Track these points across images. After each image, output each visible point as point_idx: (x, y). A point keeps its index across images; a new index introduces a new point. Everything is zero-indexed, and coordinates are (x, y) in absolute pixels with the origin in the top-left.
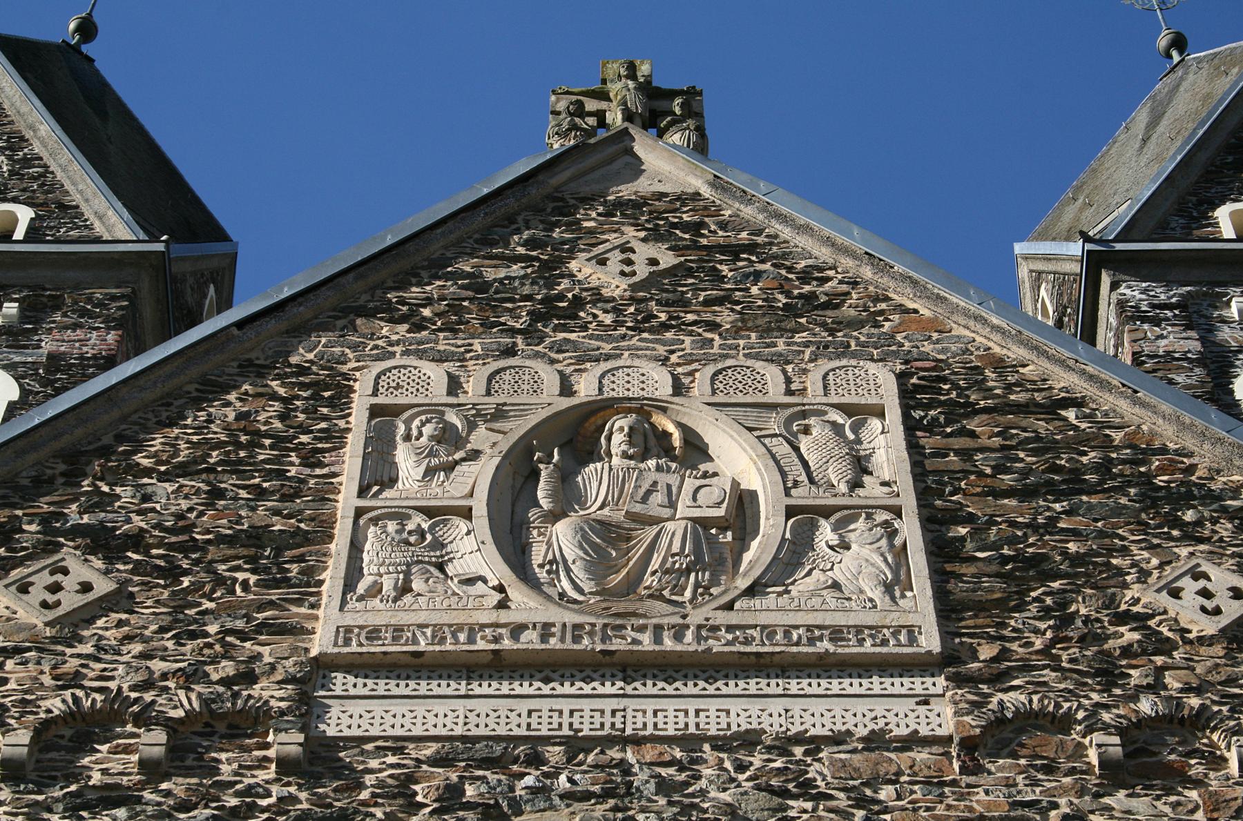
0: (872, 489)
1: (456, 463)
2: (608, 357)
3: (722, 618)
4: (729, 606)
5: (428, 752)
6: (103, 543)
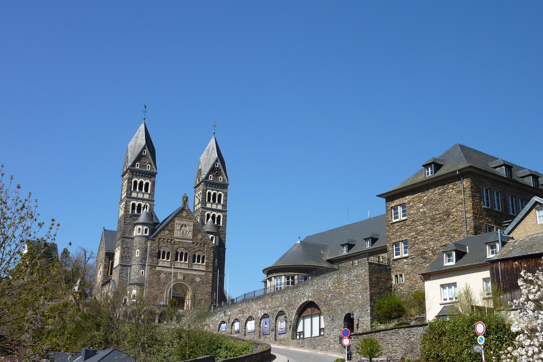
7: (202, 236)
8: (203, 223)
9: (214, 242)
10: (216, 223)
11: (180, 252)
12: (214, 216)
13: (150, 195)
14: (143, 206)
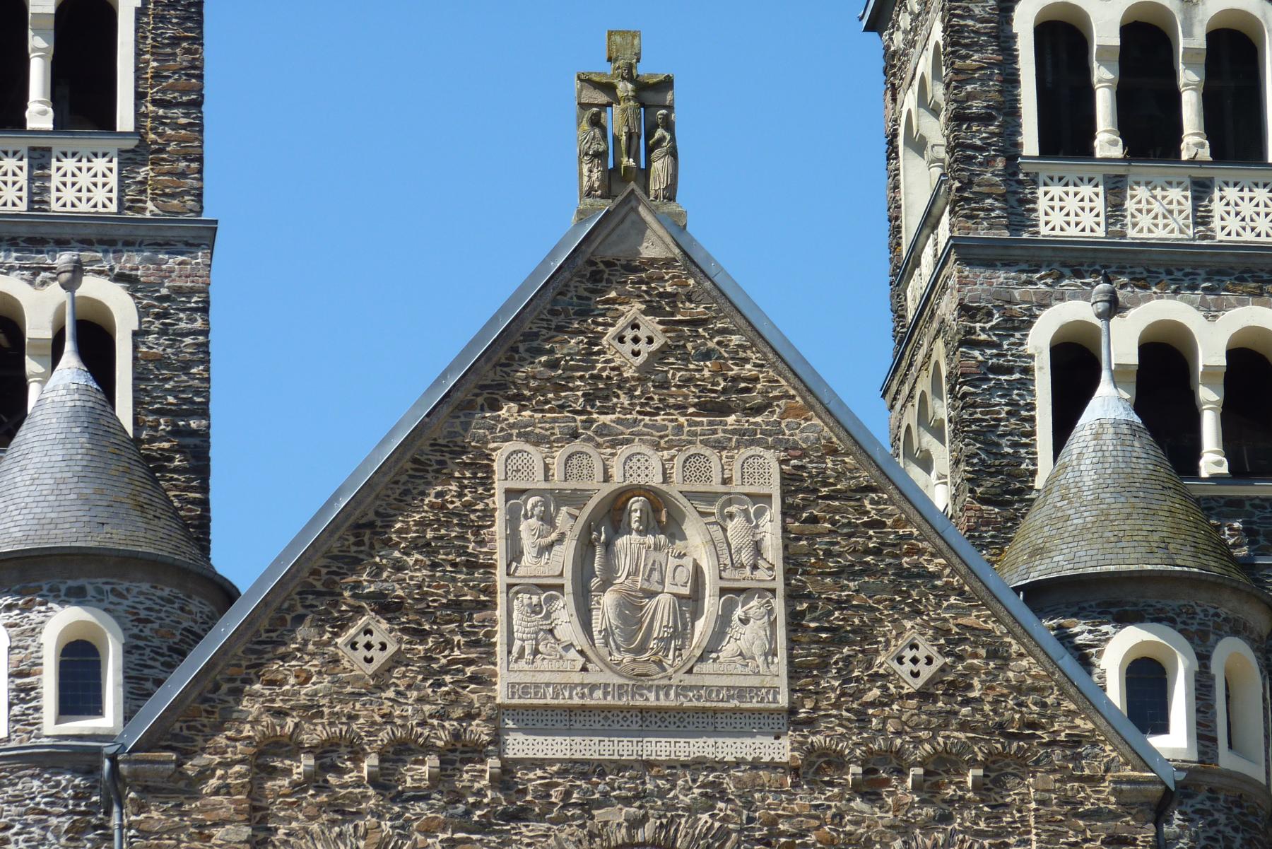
0: (761, 574)
1: (552, 545)
2: (628, 442)
3: (689, 680)
4: (690, 671)
5: (555, 768)
6: (387, 607)
7: (950, 642)
8: (1000, 486)
9: (1175, 741)
12: (1164, 362)
13: (129, 160)
14: (37, 328)
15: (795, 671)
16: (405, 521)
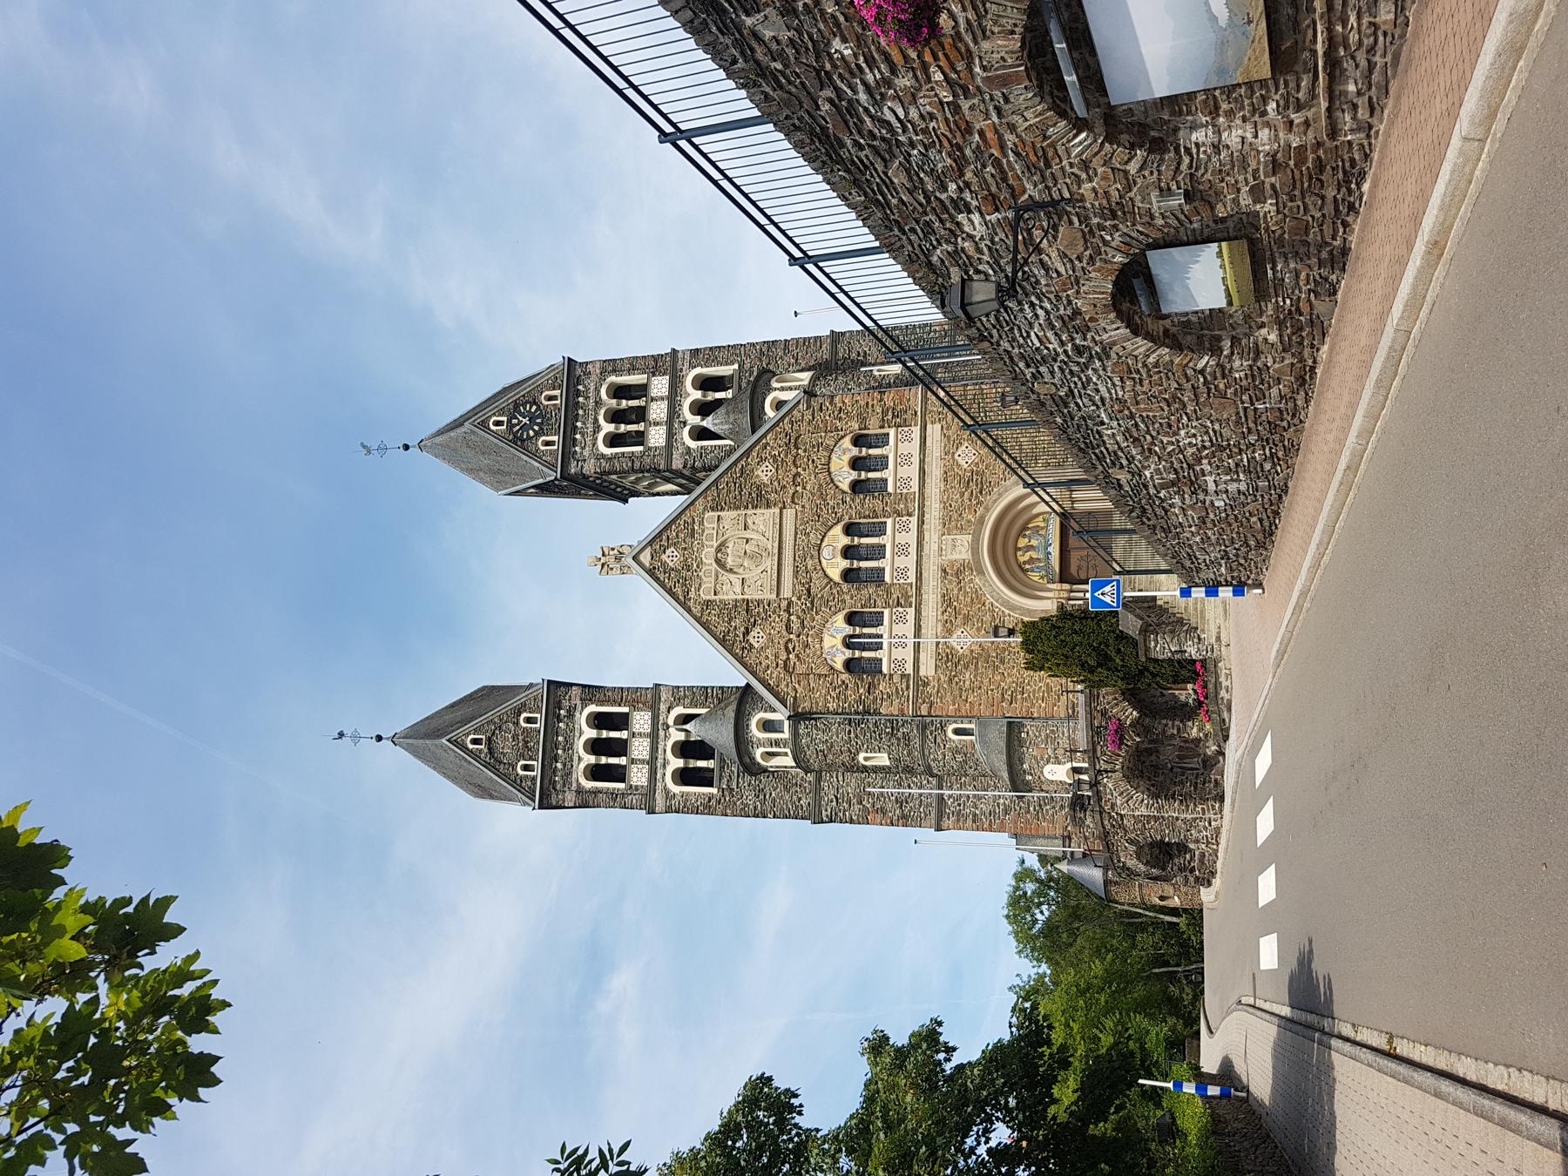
6: (747, 632)
7: (762, 460)
10: (729, 394)
11: (845, 564)
12: (703, 409)
14: (681, 736)
15: (768, 506)
16: (728, 626)
